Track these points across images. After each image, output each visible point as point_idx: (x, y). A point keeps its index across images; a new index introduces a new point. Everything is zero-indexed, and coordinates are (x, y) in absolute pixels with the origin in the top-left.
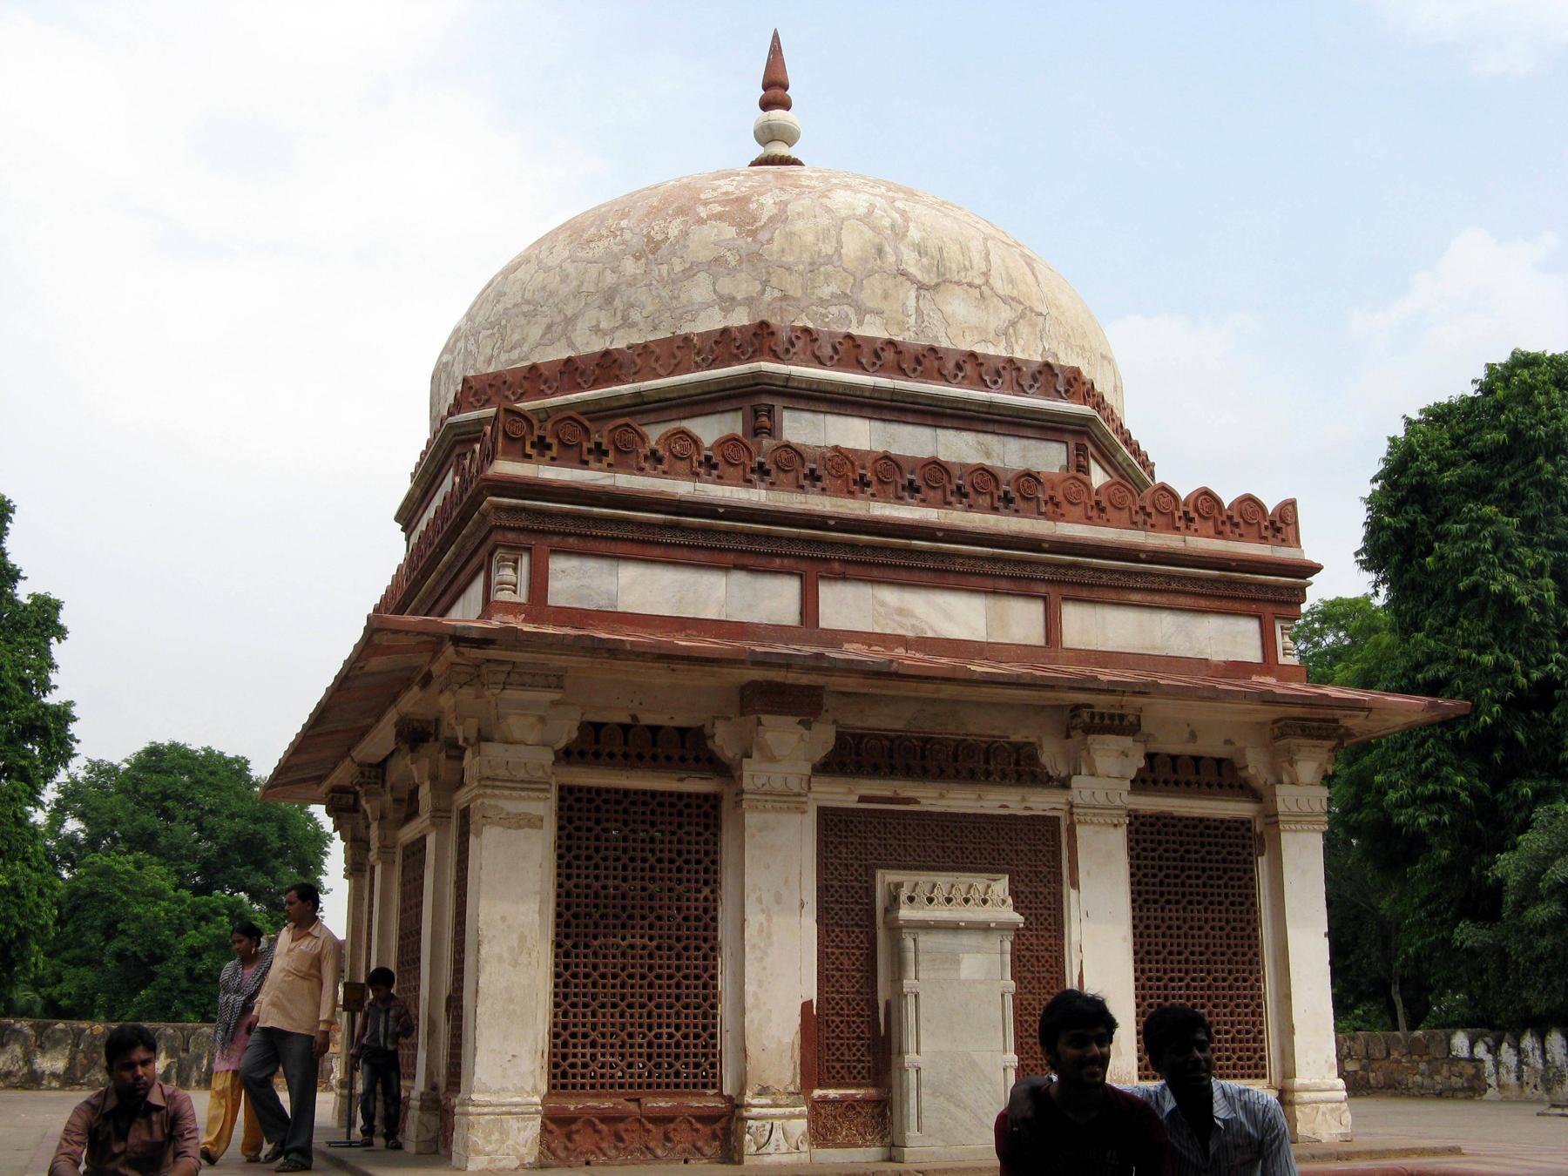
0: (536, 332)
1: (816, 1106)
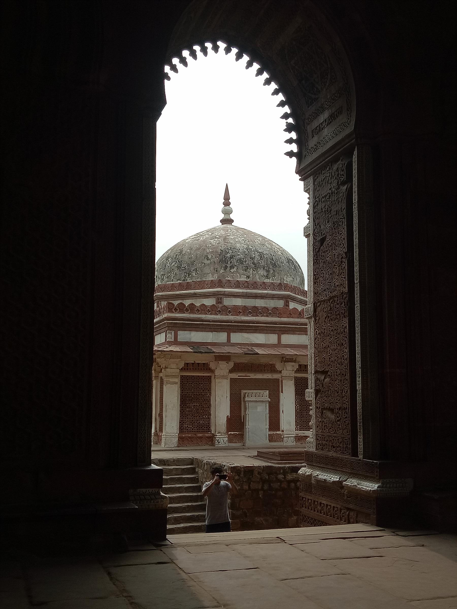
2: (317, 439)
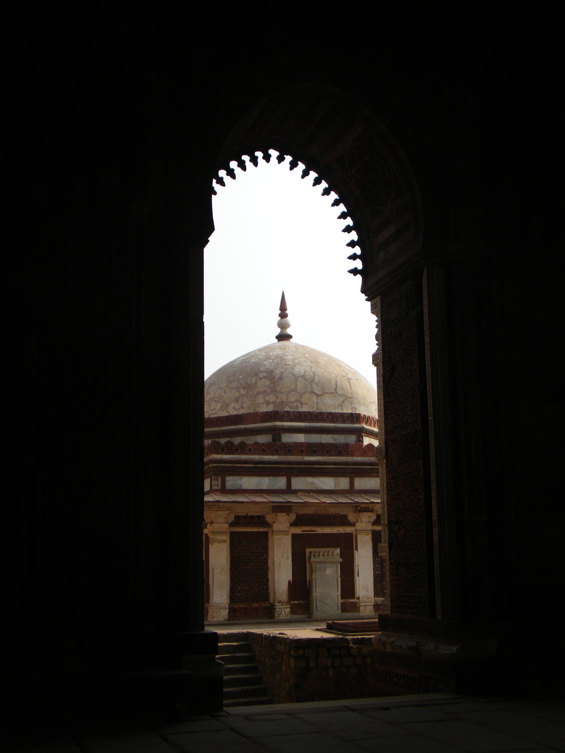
0: (218, 407)
2: (392, 601)
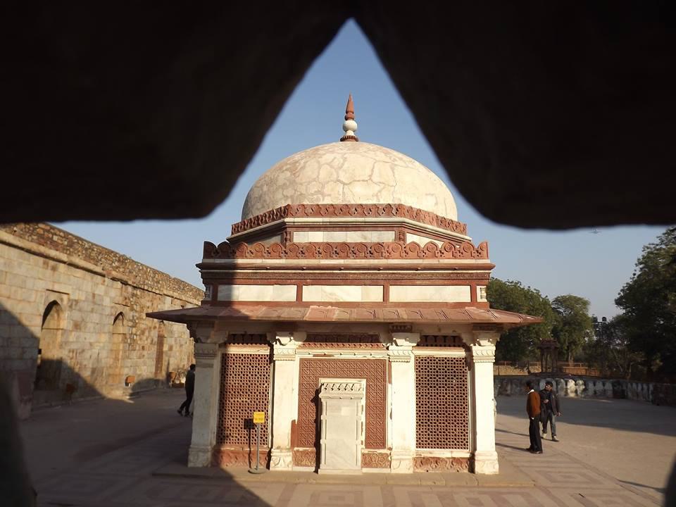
1: (295, 454)
